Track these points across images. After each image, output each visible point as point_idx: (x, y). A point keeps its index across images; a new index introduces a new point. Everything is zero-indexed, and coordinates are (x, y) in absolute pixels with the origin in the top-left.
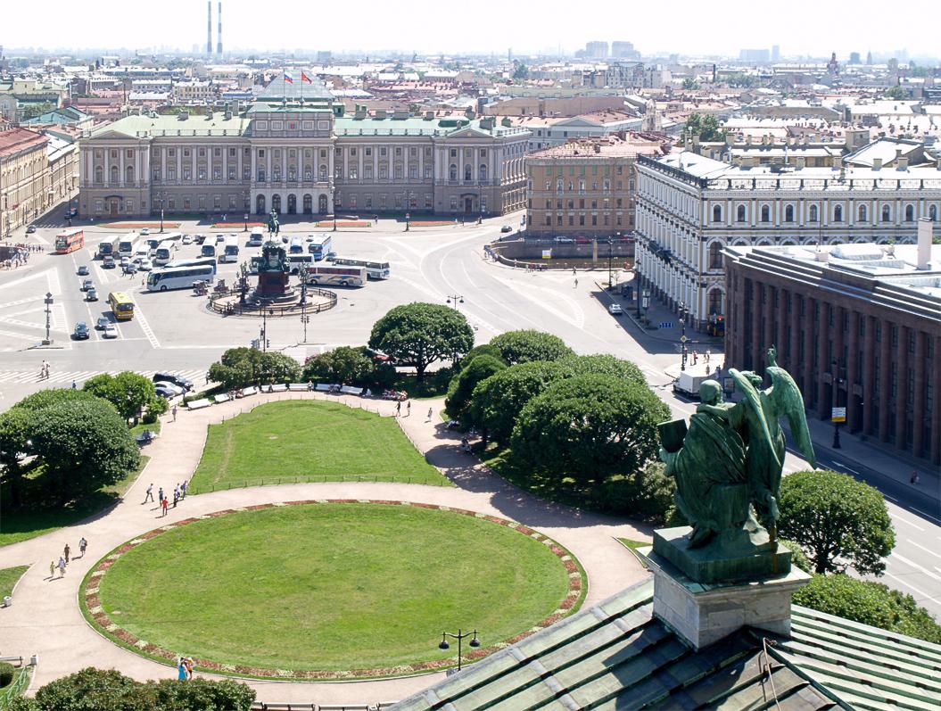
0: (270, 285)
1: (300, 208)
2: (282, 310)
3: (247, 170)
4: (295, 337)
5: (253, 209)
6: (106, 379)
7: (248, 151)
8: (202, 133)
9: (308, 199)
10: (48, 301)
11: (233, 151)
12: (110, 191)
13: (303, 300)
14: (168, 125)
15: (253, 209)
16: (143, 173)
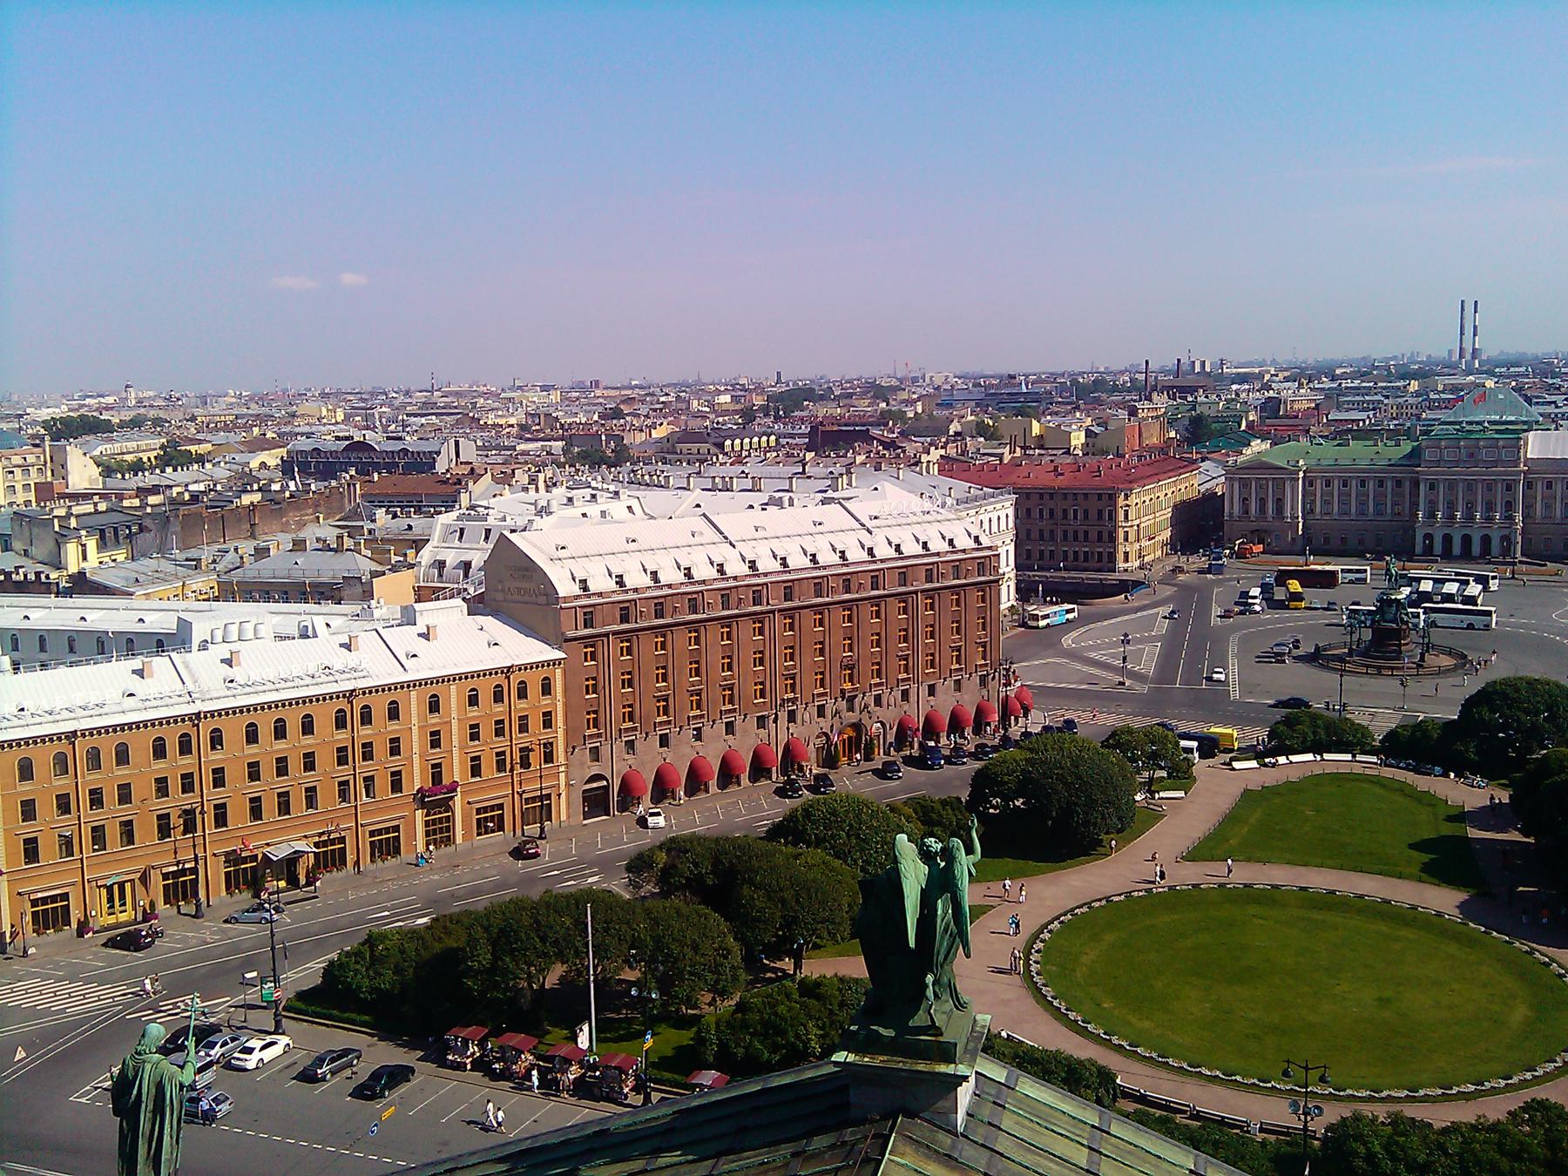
0: (1383, 641)
1: (1476, 549)
2: (1392, 669)
3: (1415, 506)
4: (1379, 706)
5: (1419, 549)
6: (1130, 731)
7: (1416, 483)
8: (1363, 463)
9: (1486, 540)
10: (1125, 642)
11: (1399, 483)
12: (1254, 526)
13: (1422, 659)
14: (1329, 452)
15: (1419, 549)
16: (1296, 507)
